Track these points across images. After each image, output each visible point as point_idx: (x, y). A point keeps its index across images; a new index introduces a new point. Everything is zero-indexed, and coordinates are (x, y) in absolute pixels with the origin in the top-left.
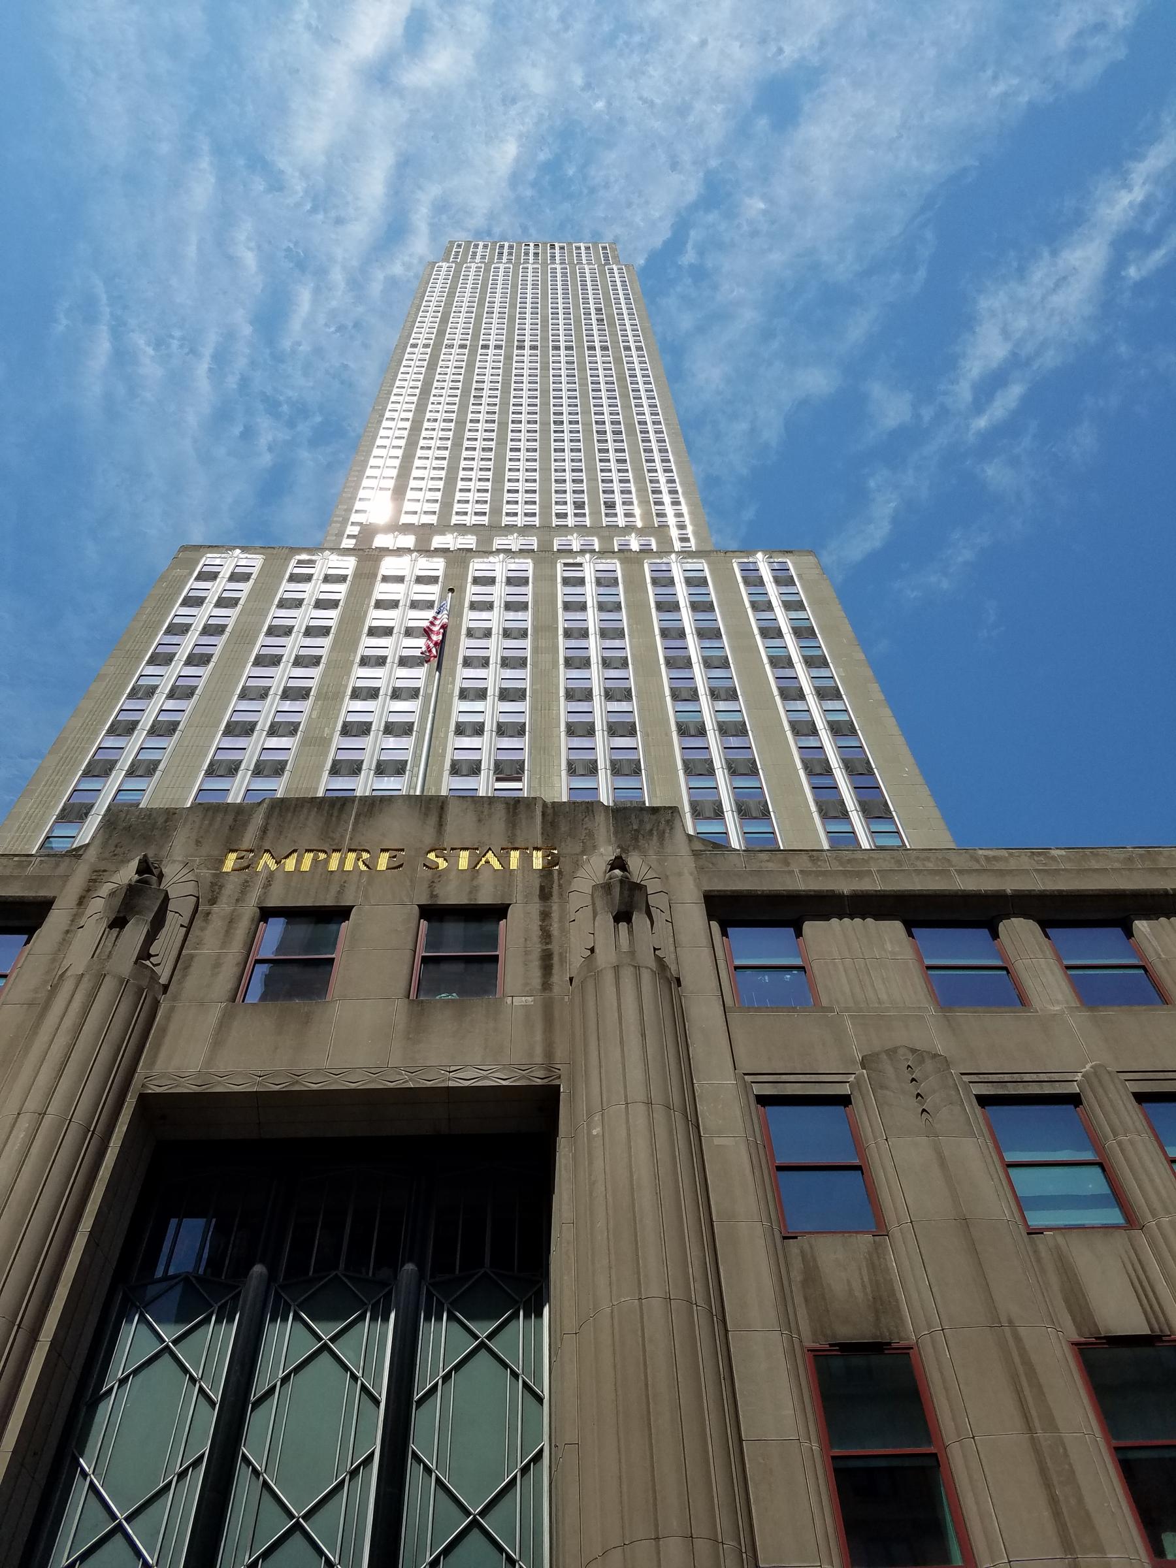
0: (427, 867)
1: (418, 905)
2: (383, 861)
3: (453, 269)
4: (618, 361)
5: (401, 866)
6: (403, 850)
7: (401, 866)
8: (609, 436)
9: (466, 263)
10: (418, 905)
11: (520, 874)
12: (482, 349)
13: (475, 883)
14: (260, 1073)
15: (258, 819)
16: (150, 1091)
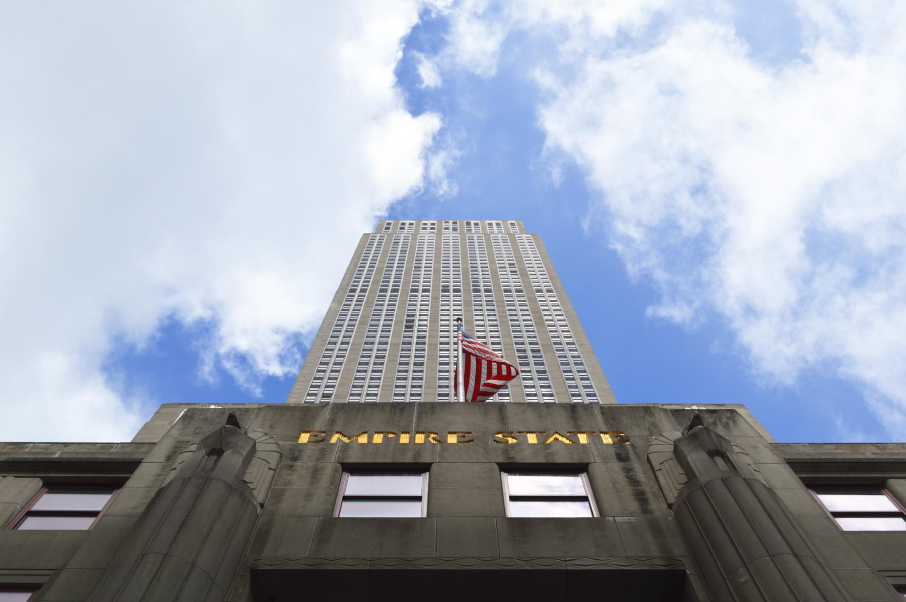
0: (497, 442)
1: (497, 463)
2: (452, 439)
3: (385, 238)
4: (532, 300)
5: (472, 441)
6: (470, 433)
7: (472, 441)
8: (530, 354)
9: (396, 234)
10: (497, 463)
11: (593, 448)
12: (411, 292)
13: (548, 451)
14: (370, 559)
15: (326, 414)
16: (261, 568)
